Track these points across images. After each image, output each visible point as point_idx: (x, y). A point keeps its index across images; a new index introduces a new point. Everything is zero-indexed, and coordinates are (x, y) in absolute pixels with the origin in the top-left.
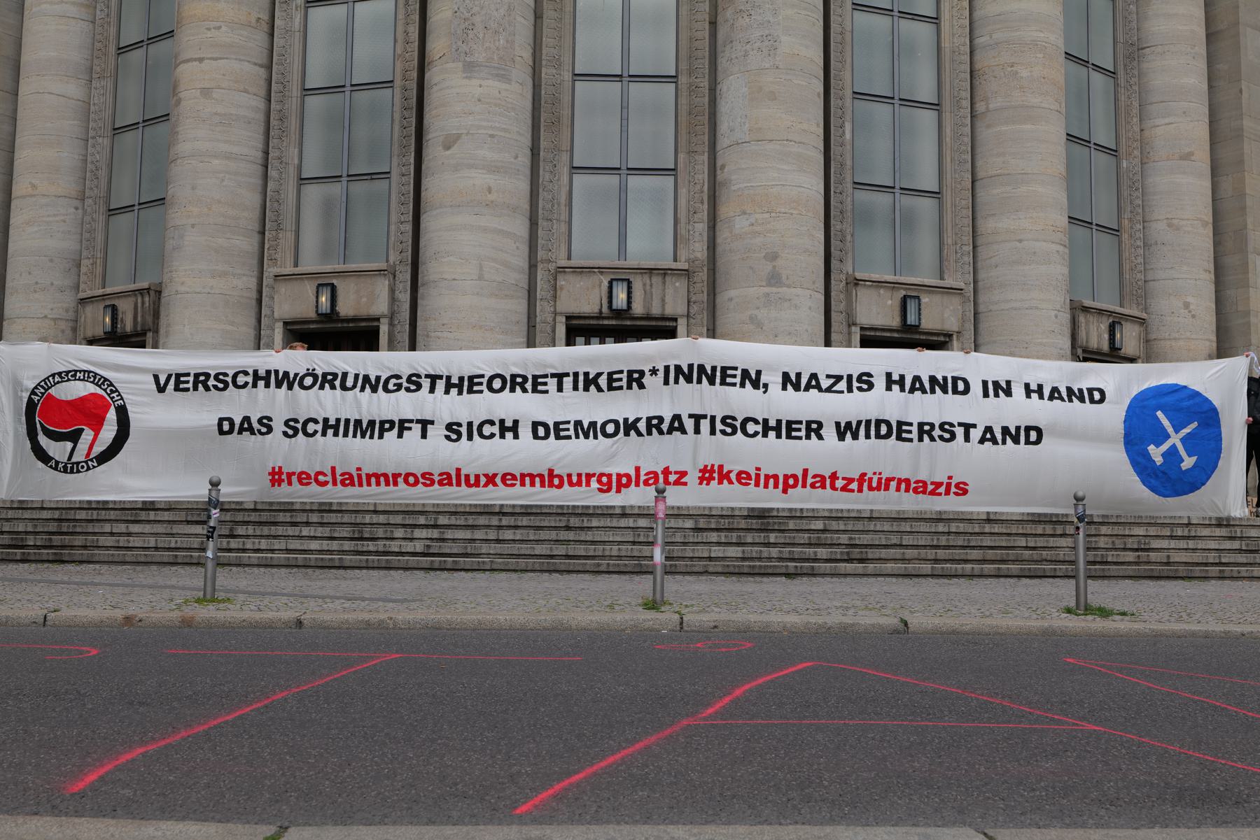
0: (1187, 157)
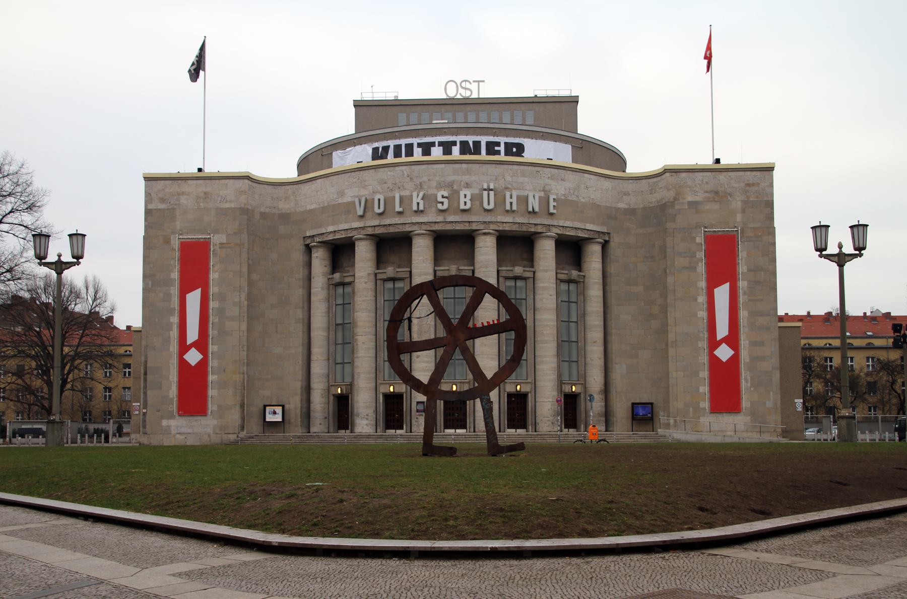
0: (595, 342)
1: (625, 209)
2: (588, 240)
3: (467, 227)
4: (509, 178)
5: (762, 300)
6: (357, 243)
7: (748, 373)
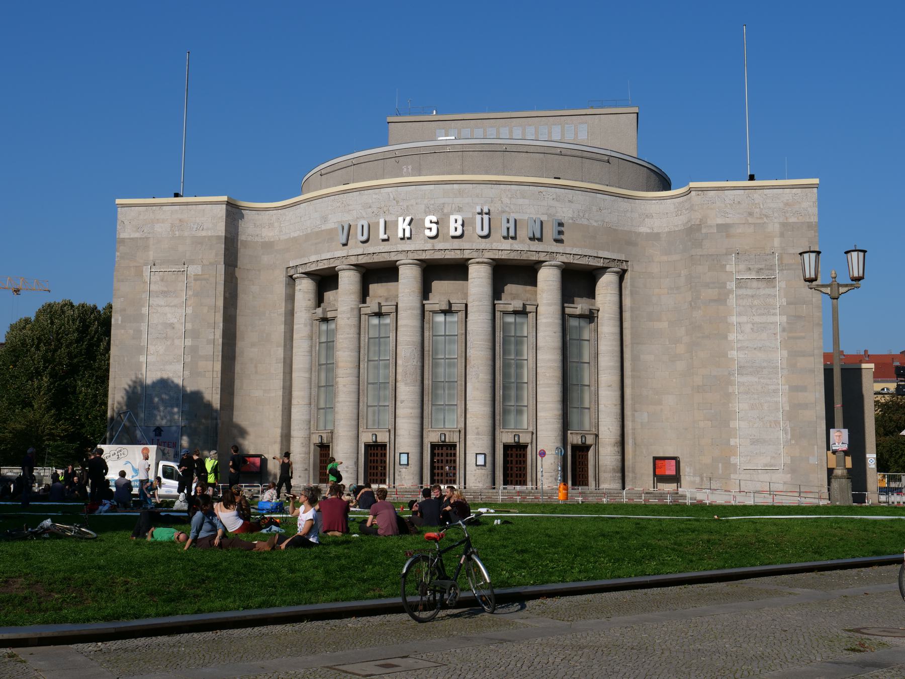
1: (647, 233)
2: (602, 270)
3: (458, 255)
4: (506, 200)
5: (804, 338)
6: (340, 274)
7: (788, 422)
